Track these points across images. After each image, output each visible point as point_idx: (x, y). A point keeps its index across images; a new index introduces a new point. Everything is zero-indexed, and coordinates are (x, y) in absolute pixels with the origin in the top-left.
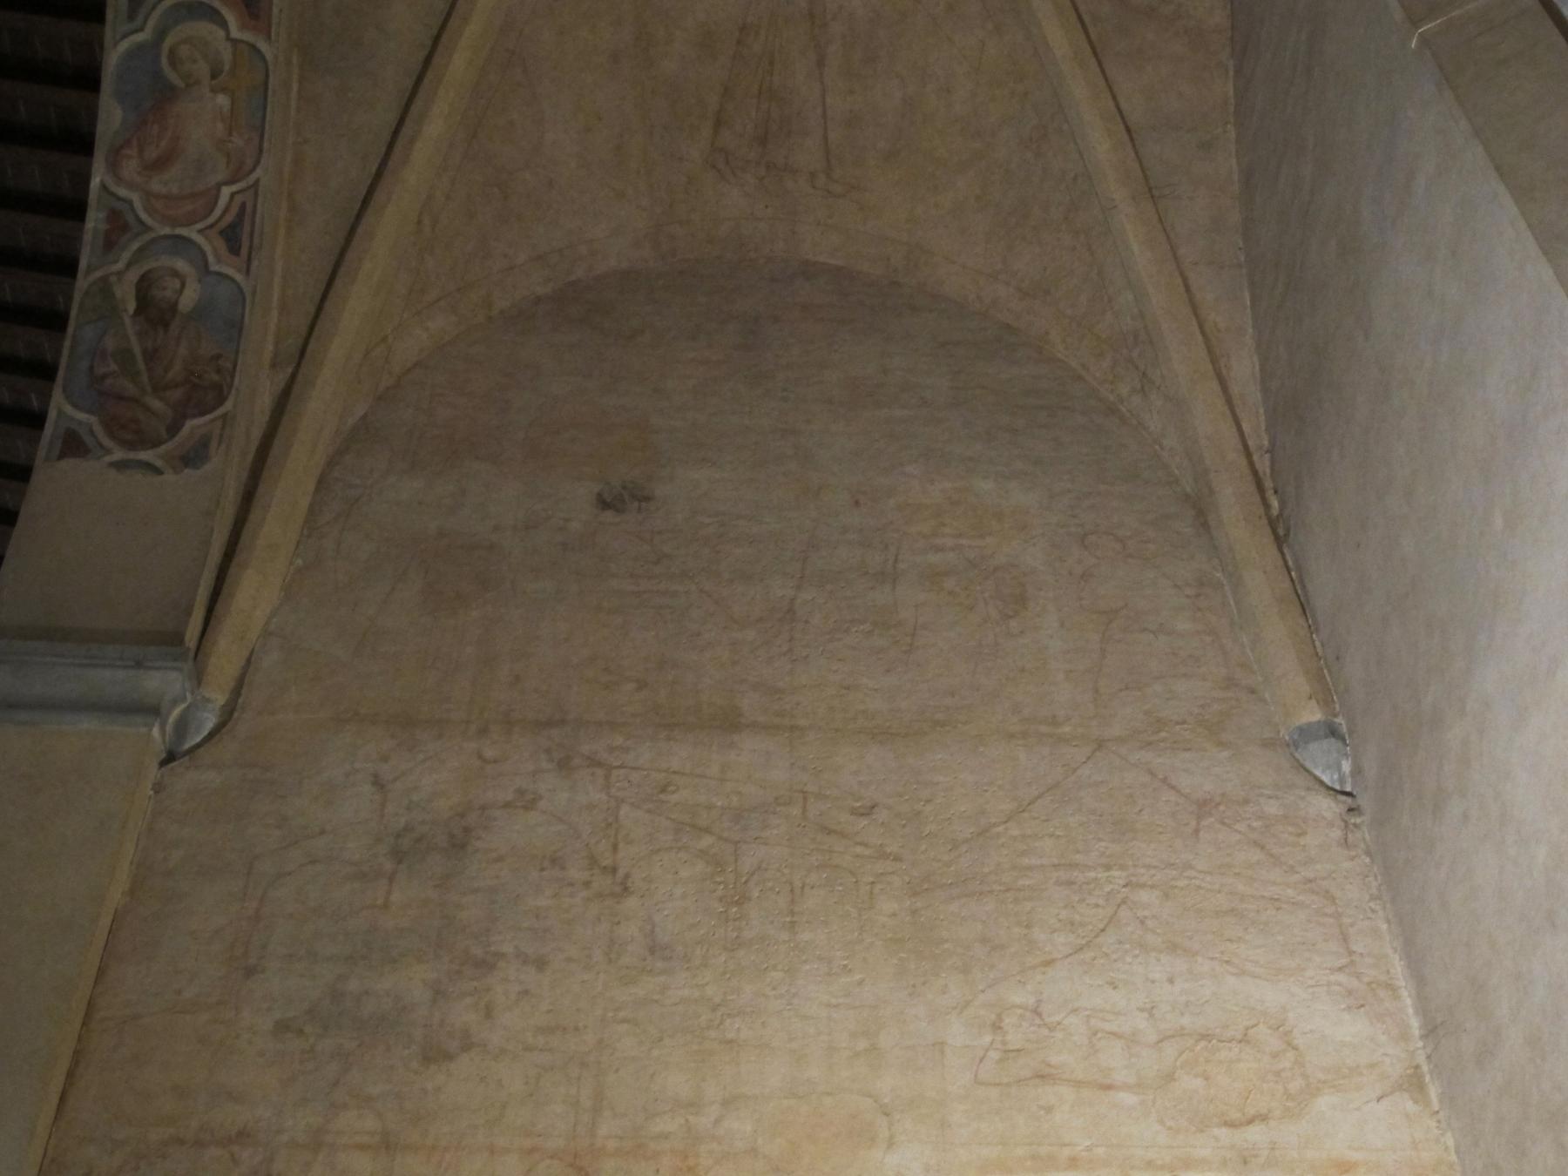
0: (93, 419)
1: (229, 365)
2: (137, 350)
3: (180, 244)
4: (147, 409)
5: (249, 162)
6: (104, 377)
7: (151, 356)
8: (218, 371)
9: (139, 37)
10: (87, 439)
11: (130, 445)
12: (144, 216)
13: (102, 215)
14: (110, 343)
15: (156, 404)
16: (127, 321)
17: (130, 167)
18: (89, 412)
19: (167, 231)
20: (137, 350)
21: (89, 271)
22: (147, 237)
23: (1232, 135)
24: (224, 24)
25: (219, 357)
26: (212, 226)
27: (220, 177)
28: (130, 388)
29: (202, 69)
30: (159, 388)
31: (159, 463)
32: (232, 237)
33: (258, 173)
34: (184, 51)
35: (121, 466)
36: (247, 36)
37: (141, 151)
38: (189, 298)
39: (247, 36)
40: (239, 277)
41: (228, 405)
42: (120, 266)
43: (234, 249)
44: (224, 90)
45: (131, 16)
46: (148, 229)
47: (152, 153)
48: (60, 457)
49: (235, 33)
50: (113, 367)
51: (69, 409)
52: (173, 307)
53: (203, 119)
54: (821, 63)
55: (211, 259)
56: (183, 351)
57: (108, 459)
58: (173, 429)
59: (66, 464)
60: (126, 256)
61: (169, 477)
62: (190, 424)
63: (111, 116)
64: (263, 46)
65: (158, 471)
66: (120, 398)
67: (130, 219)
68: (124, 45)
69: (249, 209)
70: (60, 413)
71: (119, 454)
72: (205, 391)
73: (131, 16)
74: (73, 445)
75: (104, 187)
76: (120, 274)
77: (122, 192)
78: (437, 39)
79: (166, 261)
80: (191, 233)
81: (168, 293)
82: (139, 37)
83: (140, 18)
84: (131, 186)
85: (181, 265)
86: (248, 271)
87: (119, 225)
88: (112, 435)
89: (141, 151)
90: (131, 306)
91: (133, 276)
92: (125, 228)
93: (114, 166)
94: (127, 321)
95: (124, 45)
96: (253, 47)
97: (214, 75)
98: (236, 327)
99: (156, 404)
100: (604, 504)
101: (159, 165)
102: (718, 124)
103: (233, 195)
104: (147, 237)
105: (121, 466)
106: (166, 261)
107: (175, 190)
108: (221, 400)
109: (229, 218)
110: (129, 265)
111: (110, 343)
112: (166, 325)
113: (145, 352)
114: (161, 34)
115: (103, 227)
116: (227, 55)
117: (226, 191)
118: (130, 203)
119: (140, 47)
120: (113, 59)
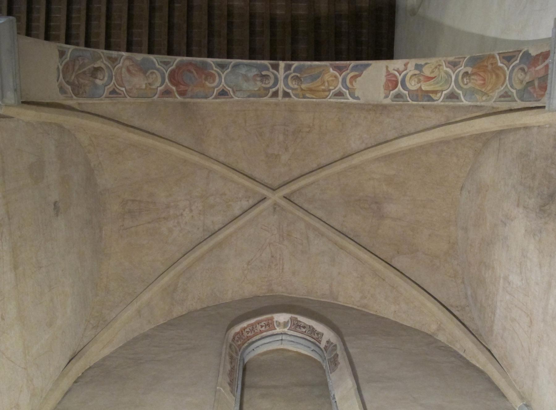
0: (68, 59)
1: (84, 96)
2: (85, 69)
3: (111, 78)
4: (72, 73)
5: (131, 95)
6: (78, 60)
7: (84, 73)
8: (82, 93)
9: (157, 65)
10: (64, 57)
11: (63, 71)
12: (117, 67)
13: (116, 56)
14: (86, 61)
15: (73, 77)
16: (92, 65)
17: (128, 63)
18: (70, 57)
19: (114, 74)
20: (85, 69)
21: (103, 53)
22: (112, 69)
23: (153, 327)
24: (161, 86)
25: (86, 92)
26: (115, 86)
27: (127, 87)
28: (77, 68)
29: (150, 81)
30: (77, 76)
31: (60, 80)
32: (113, 92)
33: (128, 97)
34: (154, 76)
35: (58, 68)
36: (158, 92)
37: (132, 65)
38: (98, 82)
39: (158, 92)
40: (104, 95)
41: (75, 97)
42: (105, 62)
43: (111, 93)
44: (146, 87)
45: (161, 62)
46: (114, 68)
47: (131, 68)
48: (59, 51)
49: (159, 89)
50: (81, 63)
51: (70, 51)
52: (96, 78)
53: (139, 81)
54: (149, 223)
55: (108, 87)
56: (87, 82)
57: (59, 64)
58: (68, 83)
59: (57, 53)
60: (107, 63)
61: (57, 84)
62: (69, 87)
63: (139, 57)
64: (157, 96)
65: (58, 80)
66: (74, 65)
67: (115, 64)
68: (155, 60)
69: (120, 96)
70: (69, 49)
71: (61, 68)
72: (77, 89)
73: (161, 62)
74: (62, 54)
75: (122, 56)
76: (103, 62)
77: (122, 60)
78: (153, 134)
79: (107, 74)
80: (114, 81)
81: (99, 76)
82: (157, 65)
83: (160, 64)
84: (123, 63)
85: (106, 79)
86: (106, 97)
87: (114, 60)
88: (65, 65)
89: (132, 65)
90: (96, 66)
91: (103, 66)
92: (113, 62)
93: (128, 58)
94: (92, 65)
95: (155, 60)
96: (156, 94)
97: (150, 84)
98: (92, 97)
99: (73, 77)
100: (55, 203)
101: (129, 71)
102: (133, 201)
103: (123, 91)
104: (112, 69)
105: (58, 68)
106: (107, 74)
107: (123, 75)
108: (76, 95)
109: (117, 90)
110: (105, 64)
111: (86, 61)
112: (91, 76)
113: (85, 71)
114: (158, 70)
115: (113, 56)
116: (154, 87)
117: (123, 89)
118: (119, 63)
119: (155, 64)
120: (152, 57)
